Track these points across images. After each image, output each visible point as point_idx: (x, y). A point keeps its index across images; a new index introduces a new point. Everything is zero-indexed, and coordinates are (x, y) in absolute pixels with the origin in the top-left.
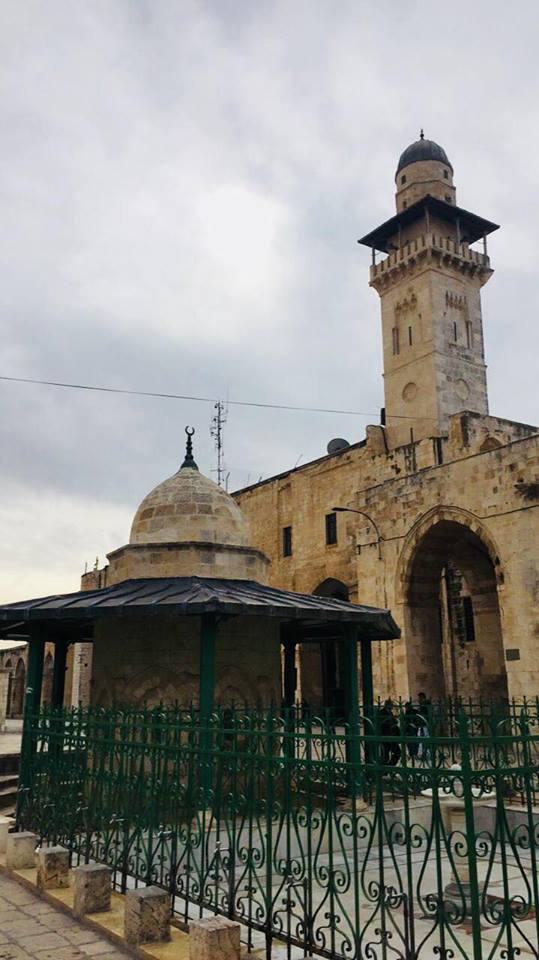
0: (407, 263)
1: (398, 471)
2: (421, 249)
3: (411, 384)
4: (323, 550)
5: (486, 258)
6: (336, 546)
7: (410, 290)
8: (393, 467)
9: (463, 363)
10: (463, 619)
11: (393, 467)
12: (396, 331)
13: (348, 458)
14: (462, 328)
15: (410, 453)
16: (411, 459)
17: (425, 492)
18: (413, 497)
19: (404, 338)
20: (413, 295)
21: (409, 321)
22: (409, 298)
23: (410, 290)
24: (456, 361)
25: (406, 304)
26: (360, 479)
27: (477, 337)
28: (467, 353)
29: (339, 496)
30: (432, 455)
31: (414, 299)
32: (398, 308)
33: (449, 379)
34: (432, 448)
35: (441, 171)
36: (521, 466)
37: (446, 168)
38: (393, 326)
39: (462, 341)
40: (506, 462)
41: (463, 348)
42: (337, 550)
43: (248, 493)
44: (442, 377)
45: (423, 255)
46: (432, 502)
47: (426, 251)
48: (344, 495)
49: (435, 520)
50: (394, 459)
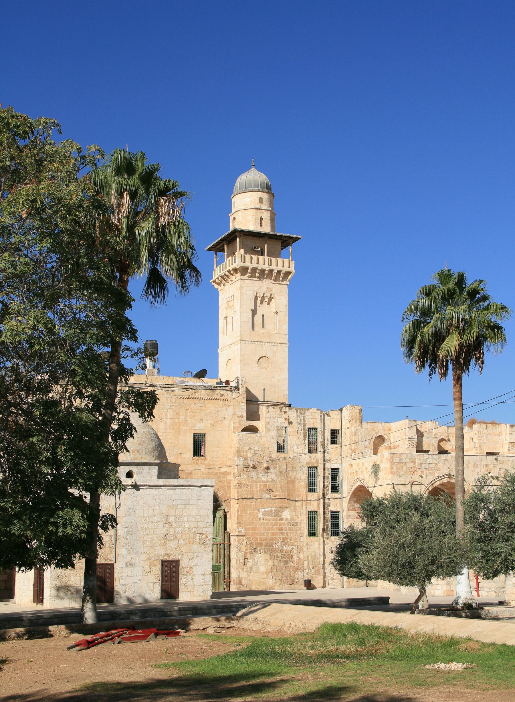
0: (275, 271)
1: (290, 423)
2: (286, 269)
4: (191, 461)
6: (206, 460)
7: (270, 290)
8: (286, 419)
10: (330, 523)
11: (286, 419)
12: (254, 312)
13: (222, 395)
15: (301, 414)
16: (302, 418)
18: (433, 466)
19: (258, 318)
20: (271, 295)
26: (233, 415)
29: (210, 422)
30: (319, 421)
32: (256, 298)
34: (319, 417)
38: (253, 308)
42: (206, 462)
47: (290, 273)
48: (217, 422)
49: (445, 480)
50: (287, 414)
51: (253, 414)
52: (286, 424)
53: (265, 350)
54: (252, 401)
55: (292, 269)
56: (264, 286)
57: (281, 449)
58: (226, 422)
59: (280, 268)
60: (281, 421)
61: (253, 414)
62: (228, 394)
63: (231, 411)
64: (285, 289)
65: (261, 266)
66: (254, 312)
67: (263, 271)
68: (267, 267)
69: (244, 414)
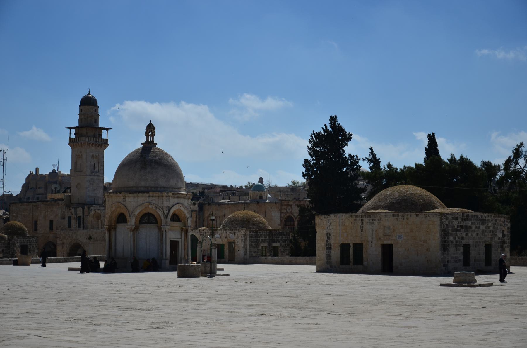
3: (79, 184)
5: (107, 140)
7: (81, 152)
9: (96, 177)
14: (97, 165)
23: (81, 152)
24: (93, 177)
27: (101, 167)
28: (98, 174)
33: (90, 184)
35: (94, 110)
37: (96, 108)
39: (97, 169)
41: (97, 172)
43: (20, 204)
44: (88, 184)
57: (70, 226)
60: (69, 214)
62: (60, 202)
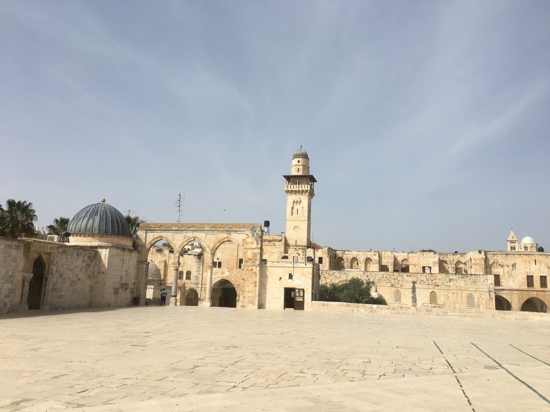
1: (299, 255)
2: (306, 189)
7: (300, 198)
12: (293, 208)
17: (342, 275)
19: (295, 211)
21: (296, 207)
22: (299, 201)
25: (297, 202)
31: (300, 202)
32: (294, 202)
36: (370, 277)
40: (366, 275)
45: (306, 191)
46: (345, 279)
51: (286, 251)
52: (297, 255)
53: (297, 224)
54: (287, 245)
55: (309, 189)
56: (296, 197)
58: (275, 254)
59: (303, 189)
61: (286, 251)
62: (277, 243)
63: (277, 250)
64: (307, 197)
65: (295, 189)
66: (293, 208)
67: (295, 191)
68: (297, 189)
69: (283, 251)
